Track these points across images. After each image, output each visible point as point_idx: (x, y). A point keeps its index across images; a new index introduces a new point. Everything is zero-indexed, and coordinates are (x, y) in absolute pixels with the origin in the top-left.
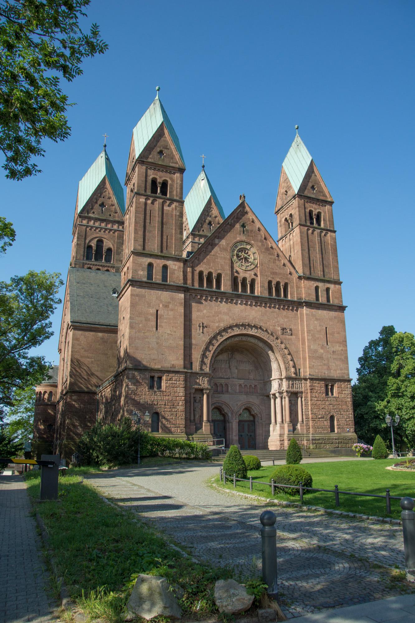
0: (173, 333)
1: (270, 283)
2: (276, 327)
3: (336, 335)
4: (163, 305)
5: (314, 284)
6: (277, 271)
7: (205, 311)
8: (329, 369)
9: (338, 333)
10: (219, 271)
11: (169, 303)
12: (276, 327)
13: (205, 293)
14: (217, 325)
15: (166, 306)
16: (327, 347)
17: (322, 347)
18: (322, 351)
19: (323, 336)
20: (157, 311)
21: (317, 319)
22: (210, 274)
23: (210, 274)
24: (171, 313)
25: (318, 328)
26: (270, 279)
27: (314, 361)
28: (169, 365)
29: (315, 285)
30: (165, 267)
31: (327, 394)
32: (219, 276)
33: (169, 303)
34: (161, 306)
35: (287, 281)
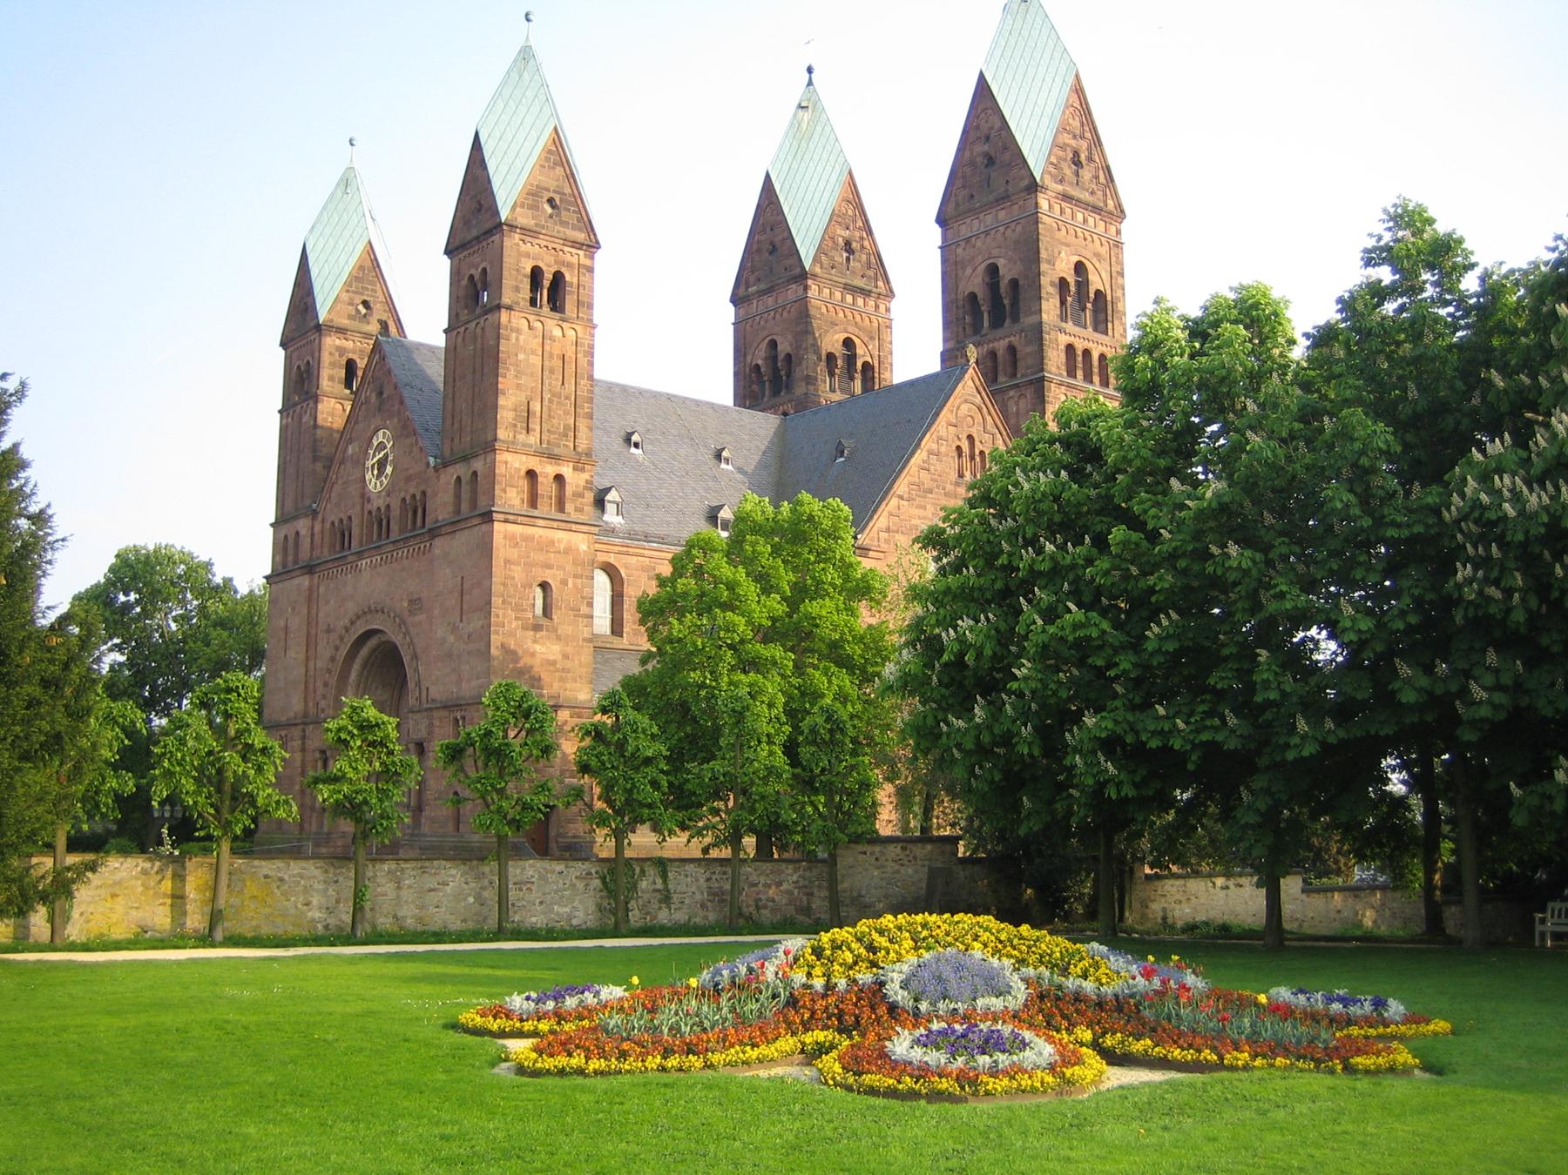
28: (292, 715)
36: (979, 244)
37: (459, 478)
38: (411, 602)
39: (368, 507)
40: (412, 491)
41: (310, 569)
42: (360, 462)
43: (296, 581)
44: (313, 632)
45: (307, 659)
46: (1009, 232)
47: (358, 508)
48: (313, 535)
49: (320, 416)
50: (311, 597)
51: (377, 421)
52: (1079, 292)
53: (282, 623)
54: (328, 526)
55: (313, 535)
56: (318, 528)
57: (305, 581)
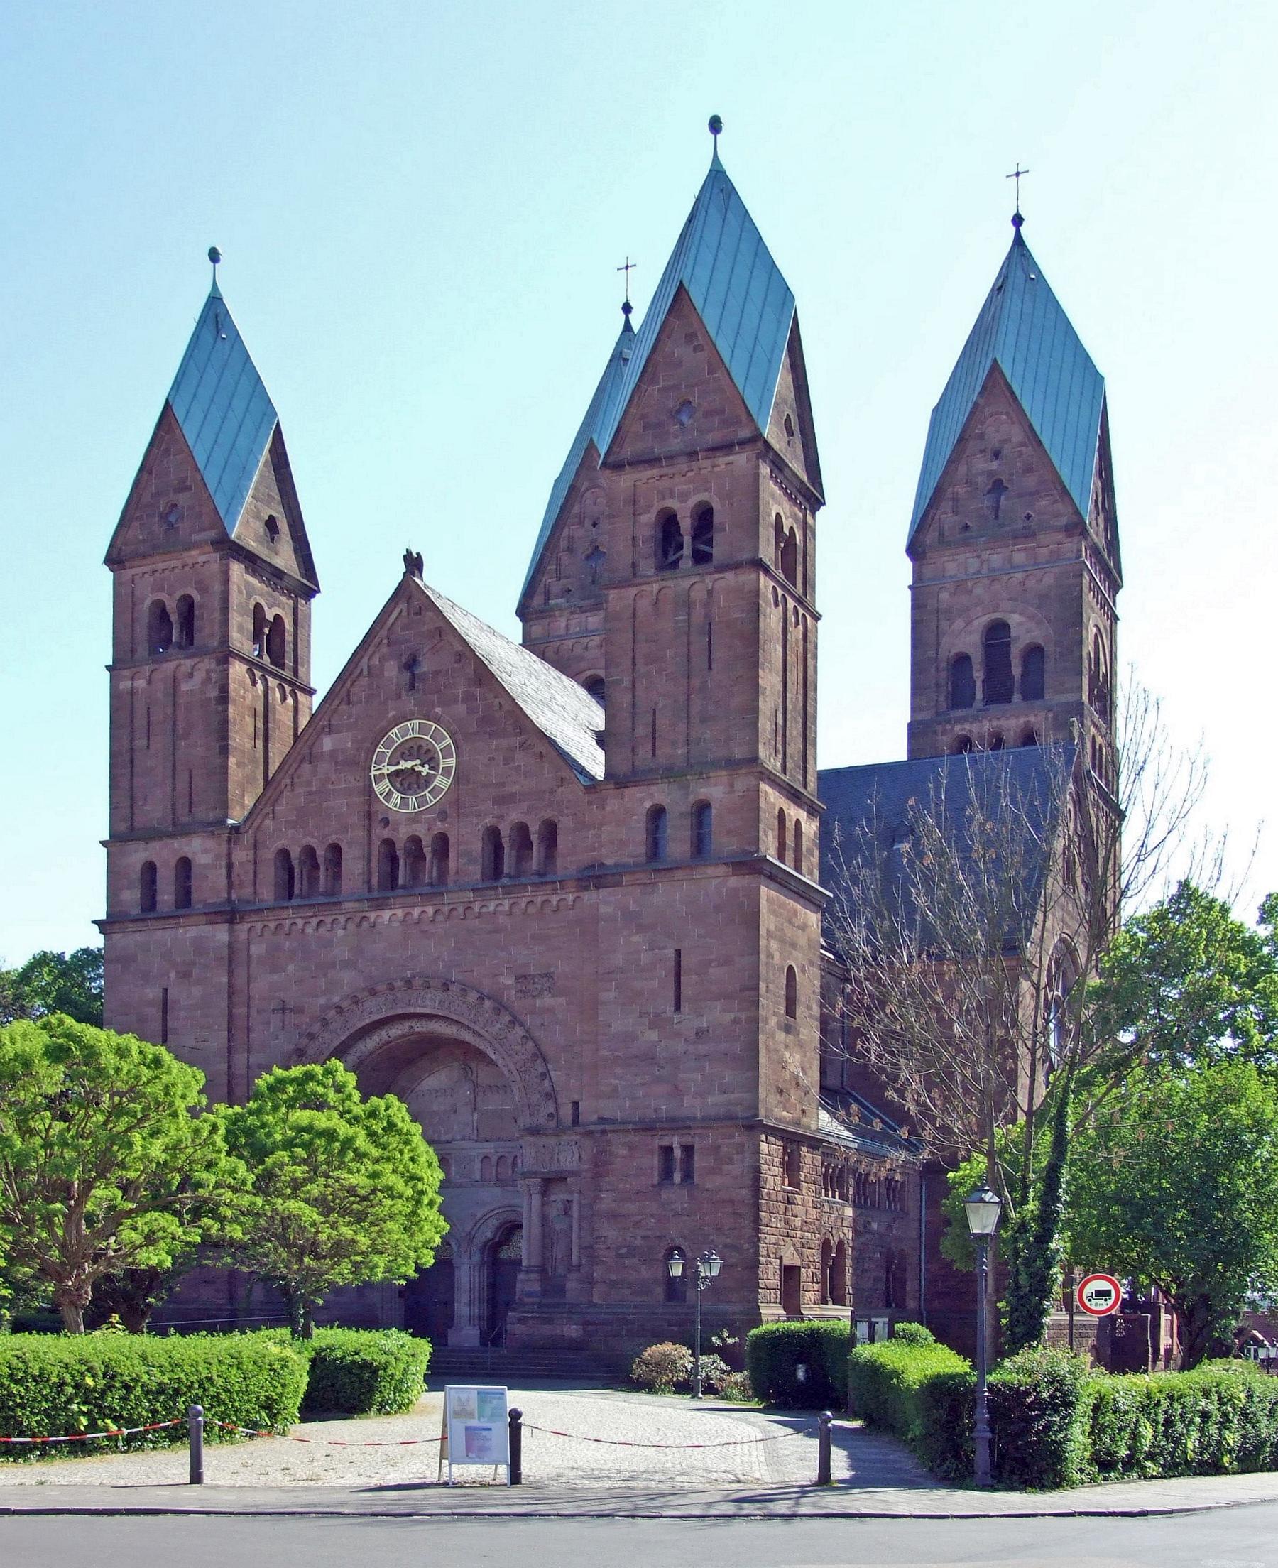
0: (200, 1045)
1: (493, 836)
2: (502, 979)
3: (714, 971)
4: (177, 973)
5: (642, 800)
6: (515, 789)
7: (291, 968)
8: (677, 1092)
9: (727, 961)
10: (332, 839)
11: (193, 963)
12: (502, 979)
13: (285, 913)
14: (322, 1001)
15: (185, 975)
16: (677, 1017)
17: (657, 1022)
18: (654, 1036)
19: (660, 980)
20: (166, 990)
21: (641, 928)
22: (310, 852)
23: (310, 852)
24: (197, 991)
25: (646, 958)
26: (489, 821)
27: (619, 1071)
29: (648, 805)
30: (185, 865)
31: (667, 1174)
32: (336, 850)
33: (193, 963)
34: (173, 975)
35: (548, 814)
36: (978, 591)
37: (657, 814)
38: (522, 978)
39: (386, 833)
40: (515, 815)
41: (230, 914)
42: (360, 762)
43: (192, 932)
44: (241, 1011)
45: (230, 1050)
46: (1031, 583)
47: (360, 833)
48: (230, 866)
49: (232, 686)
50: (232, 957)
51: (409, 703)
52: (990, 671)
53: (153, 993)
54: (269, 854)
55: (230, 866)
56: (241, 855)
57: (221, 934)
